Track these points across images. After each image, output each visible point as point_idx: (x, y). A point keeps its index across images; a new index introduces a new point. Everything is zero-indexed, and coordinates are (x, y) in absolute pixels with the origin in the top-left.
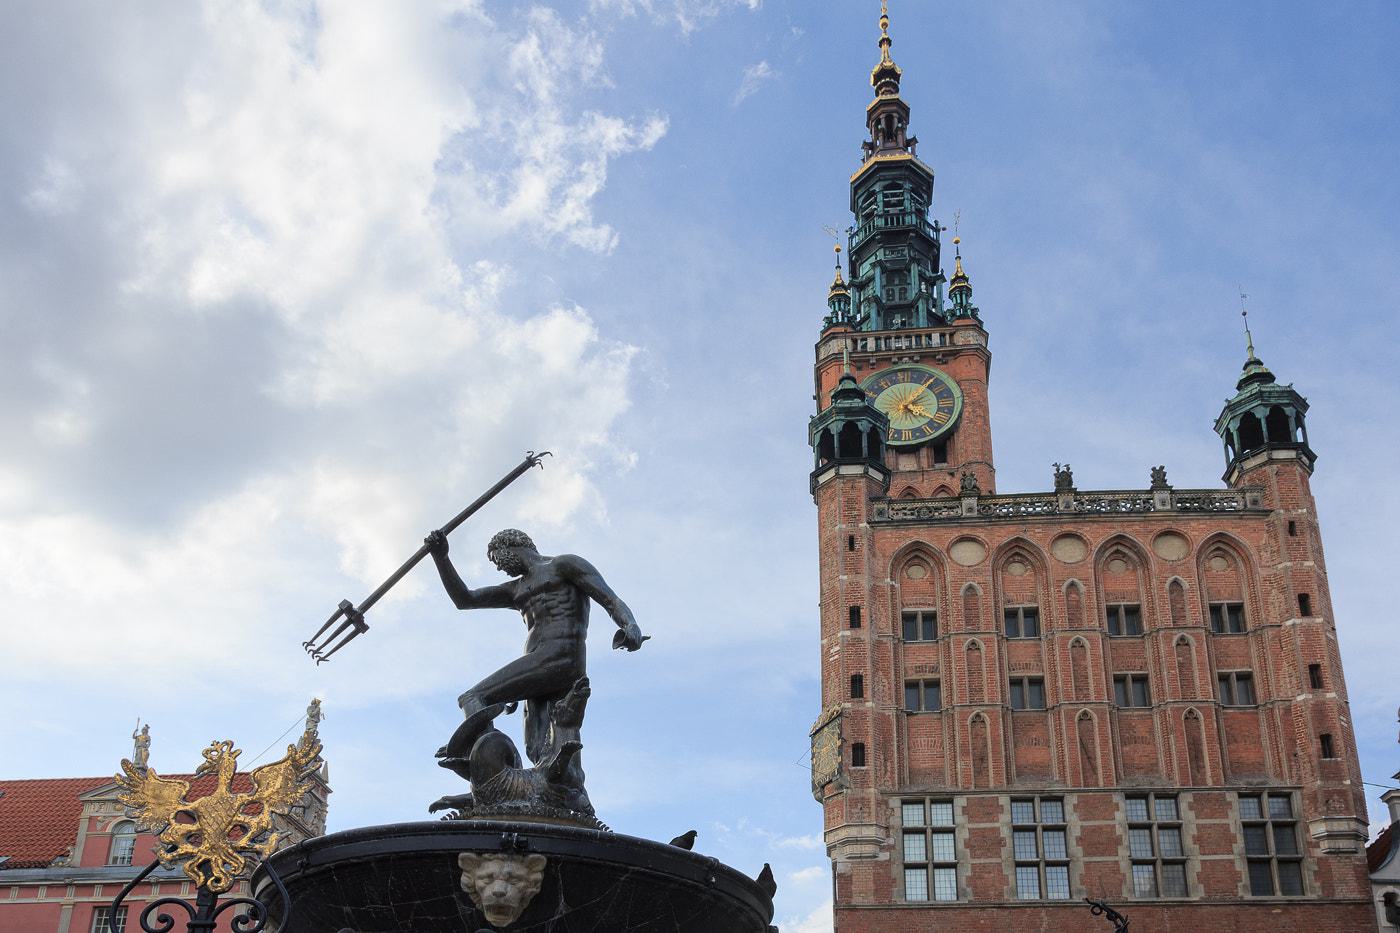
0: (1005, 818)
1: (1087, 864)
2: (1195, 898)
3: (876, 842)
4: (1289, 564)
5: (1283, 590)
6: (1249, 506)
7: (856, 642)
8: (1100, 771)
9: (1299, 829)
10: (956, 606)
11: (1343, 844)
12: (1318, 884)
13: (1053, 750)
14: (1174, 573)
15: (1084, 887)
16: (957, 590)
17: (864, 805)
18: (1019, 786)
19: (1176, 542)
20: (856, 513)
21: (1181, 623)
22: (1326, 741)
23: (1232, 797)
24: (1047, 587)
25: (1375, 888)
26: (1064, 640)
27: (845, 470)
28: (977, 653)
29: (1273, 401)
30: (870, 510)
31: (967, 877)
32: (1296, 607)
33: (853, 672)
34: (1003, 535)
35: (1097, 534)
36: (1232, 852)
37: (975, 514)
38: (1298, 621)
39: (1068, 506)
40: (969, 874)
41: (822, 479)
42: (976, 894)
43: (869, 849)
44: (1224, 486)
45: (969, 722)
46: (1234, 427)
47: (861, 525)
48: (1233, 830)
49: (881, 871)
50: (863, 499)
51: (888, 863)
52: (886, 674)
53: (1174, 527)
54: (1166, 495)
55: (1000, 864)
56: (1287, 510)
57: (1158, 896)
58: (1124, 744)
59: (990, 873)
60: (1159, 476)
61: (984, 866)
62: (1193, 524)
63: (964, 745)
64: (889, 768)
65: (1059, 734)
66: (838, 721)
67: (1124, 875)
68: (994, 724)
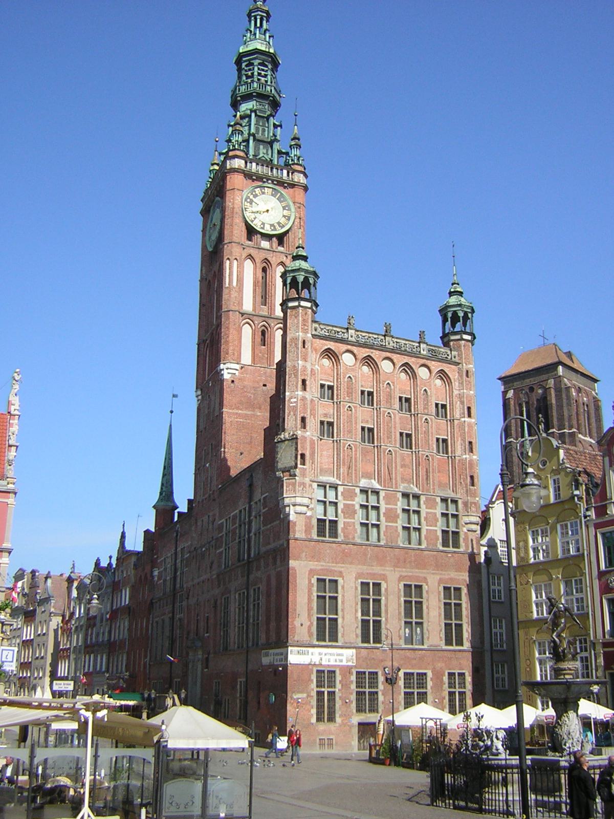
0: (357, 499)
1: (386, 526)
2: (423, 547)
3: (308, 506)
5: (462, 403)
6: (453, 359)
8: (394, 481)
9: (460, 517)
10: (344, 387)
11: (474, 527)
12: (464, 544)
13: (376, 467)
14: (425, 386)
15: (384, 537)
16: (344, 378)
17: (304, 486)
18: (364, 483)
19: (426, 369)
20: (306, 328)
21: (426, 411)
22: (472, 477)
23: (438, 500)
25: (481, 547)
26: (384, 412)
27: (303, 303)
28: (350, 412)
29: (465, 309)
30: (312, 327)
31: (343, 529)
33: (302, 415)
34: (363, 352)
35: (400, 360)
36: (436, 526)
37: (353, 339)
38: (467, 419)
39: (389, 344)
40: (342, 526)
41: (291, 304)
42: (344, 537)
43: (304, 509)
44: (440, 343)
45: (346, 449)
46: (450, 315)
48: (438, 516)
50: (310, 321)
51: (311, 517)
52: (314, 417)
53: (428, 363)
54: (425, 345)
55: (354, 523)
56: (466, 364)
57: (410, 543)
58: (402, 467)
60: (422, 334)
61: (348, 522)
62: (433, 362)
63: (344, 459)
66: (294, 441)
68: (356, 451)
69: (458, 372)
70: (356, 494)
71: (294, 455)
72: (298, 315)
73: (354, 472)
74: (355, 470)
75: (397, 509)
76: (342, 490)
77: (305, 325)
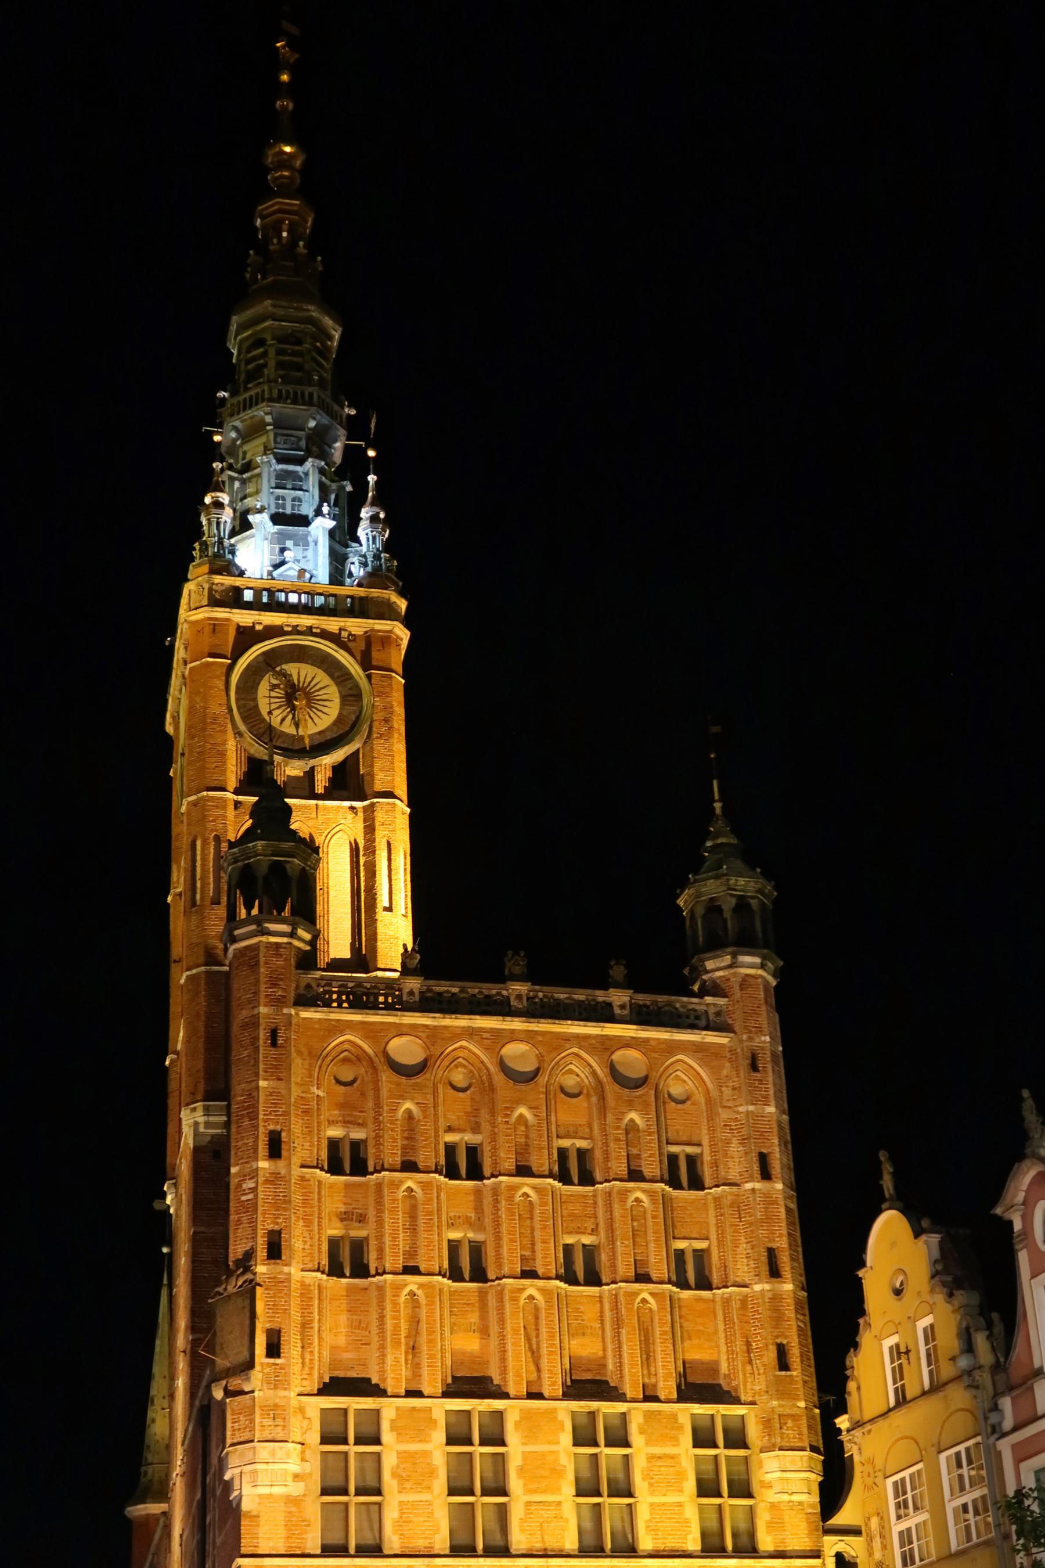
1: (528, 1504)
4: (751, 1108)
5: (744, 1141)
7: (275, 1179)
13: (494, 1342)
24: (493, 1113)
31: (395, 1522)
32: (756, 1167)
38: (758, 1185)
40: (395, 1515)
47: (285, 1011)
49: (294, 1509)
55: (430, 1503)
59: (417, 1515)
61: (414, 1504)
64: (307, 1361)
65: (502, 1321)
67: (567, 1521)
68: (431, 1303)
69: (730, 1060)
70: (435, 1422)
71: (247, 1330)
72: (257, 963)
73: (425, 1362)
74: (431, 1357)
75: (557, 1453)
76: (394, 1417)
77: (274, 985)
